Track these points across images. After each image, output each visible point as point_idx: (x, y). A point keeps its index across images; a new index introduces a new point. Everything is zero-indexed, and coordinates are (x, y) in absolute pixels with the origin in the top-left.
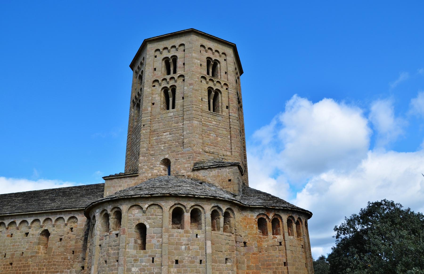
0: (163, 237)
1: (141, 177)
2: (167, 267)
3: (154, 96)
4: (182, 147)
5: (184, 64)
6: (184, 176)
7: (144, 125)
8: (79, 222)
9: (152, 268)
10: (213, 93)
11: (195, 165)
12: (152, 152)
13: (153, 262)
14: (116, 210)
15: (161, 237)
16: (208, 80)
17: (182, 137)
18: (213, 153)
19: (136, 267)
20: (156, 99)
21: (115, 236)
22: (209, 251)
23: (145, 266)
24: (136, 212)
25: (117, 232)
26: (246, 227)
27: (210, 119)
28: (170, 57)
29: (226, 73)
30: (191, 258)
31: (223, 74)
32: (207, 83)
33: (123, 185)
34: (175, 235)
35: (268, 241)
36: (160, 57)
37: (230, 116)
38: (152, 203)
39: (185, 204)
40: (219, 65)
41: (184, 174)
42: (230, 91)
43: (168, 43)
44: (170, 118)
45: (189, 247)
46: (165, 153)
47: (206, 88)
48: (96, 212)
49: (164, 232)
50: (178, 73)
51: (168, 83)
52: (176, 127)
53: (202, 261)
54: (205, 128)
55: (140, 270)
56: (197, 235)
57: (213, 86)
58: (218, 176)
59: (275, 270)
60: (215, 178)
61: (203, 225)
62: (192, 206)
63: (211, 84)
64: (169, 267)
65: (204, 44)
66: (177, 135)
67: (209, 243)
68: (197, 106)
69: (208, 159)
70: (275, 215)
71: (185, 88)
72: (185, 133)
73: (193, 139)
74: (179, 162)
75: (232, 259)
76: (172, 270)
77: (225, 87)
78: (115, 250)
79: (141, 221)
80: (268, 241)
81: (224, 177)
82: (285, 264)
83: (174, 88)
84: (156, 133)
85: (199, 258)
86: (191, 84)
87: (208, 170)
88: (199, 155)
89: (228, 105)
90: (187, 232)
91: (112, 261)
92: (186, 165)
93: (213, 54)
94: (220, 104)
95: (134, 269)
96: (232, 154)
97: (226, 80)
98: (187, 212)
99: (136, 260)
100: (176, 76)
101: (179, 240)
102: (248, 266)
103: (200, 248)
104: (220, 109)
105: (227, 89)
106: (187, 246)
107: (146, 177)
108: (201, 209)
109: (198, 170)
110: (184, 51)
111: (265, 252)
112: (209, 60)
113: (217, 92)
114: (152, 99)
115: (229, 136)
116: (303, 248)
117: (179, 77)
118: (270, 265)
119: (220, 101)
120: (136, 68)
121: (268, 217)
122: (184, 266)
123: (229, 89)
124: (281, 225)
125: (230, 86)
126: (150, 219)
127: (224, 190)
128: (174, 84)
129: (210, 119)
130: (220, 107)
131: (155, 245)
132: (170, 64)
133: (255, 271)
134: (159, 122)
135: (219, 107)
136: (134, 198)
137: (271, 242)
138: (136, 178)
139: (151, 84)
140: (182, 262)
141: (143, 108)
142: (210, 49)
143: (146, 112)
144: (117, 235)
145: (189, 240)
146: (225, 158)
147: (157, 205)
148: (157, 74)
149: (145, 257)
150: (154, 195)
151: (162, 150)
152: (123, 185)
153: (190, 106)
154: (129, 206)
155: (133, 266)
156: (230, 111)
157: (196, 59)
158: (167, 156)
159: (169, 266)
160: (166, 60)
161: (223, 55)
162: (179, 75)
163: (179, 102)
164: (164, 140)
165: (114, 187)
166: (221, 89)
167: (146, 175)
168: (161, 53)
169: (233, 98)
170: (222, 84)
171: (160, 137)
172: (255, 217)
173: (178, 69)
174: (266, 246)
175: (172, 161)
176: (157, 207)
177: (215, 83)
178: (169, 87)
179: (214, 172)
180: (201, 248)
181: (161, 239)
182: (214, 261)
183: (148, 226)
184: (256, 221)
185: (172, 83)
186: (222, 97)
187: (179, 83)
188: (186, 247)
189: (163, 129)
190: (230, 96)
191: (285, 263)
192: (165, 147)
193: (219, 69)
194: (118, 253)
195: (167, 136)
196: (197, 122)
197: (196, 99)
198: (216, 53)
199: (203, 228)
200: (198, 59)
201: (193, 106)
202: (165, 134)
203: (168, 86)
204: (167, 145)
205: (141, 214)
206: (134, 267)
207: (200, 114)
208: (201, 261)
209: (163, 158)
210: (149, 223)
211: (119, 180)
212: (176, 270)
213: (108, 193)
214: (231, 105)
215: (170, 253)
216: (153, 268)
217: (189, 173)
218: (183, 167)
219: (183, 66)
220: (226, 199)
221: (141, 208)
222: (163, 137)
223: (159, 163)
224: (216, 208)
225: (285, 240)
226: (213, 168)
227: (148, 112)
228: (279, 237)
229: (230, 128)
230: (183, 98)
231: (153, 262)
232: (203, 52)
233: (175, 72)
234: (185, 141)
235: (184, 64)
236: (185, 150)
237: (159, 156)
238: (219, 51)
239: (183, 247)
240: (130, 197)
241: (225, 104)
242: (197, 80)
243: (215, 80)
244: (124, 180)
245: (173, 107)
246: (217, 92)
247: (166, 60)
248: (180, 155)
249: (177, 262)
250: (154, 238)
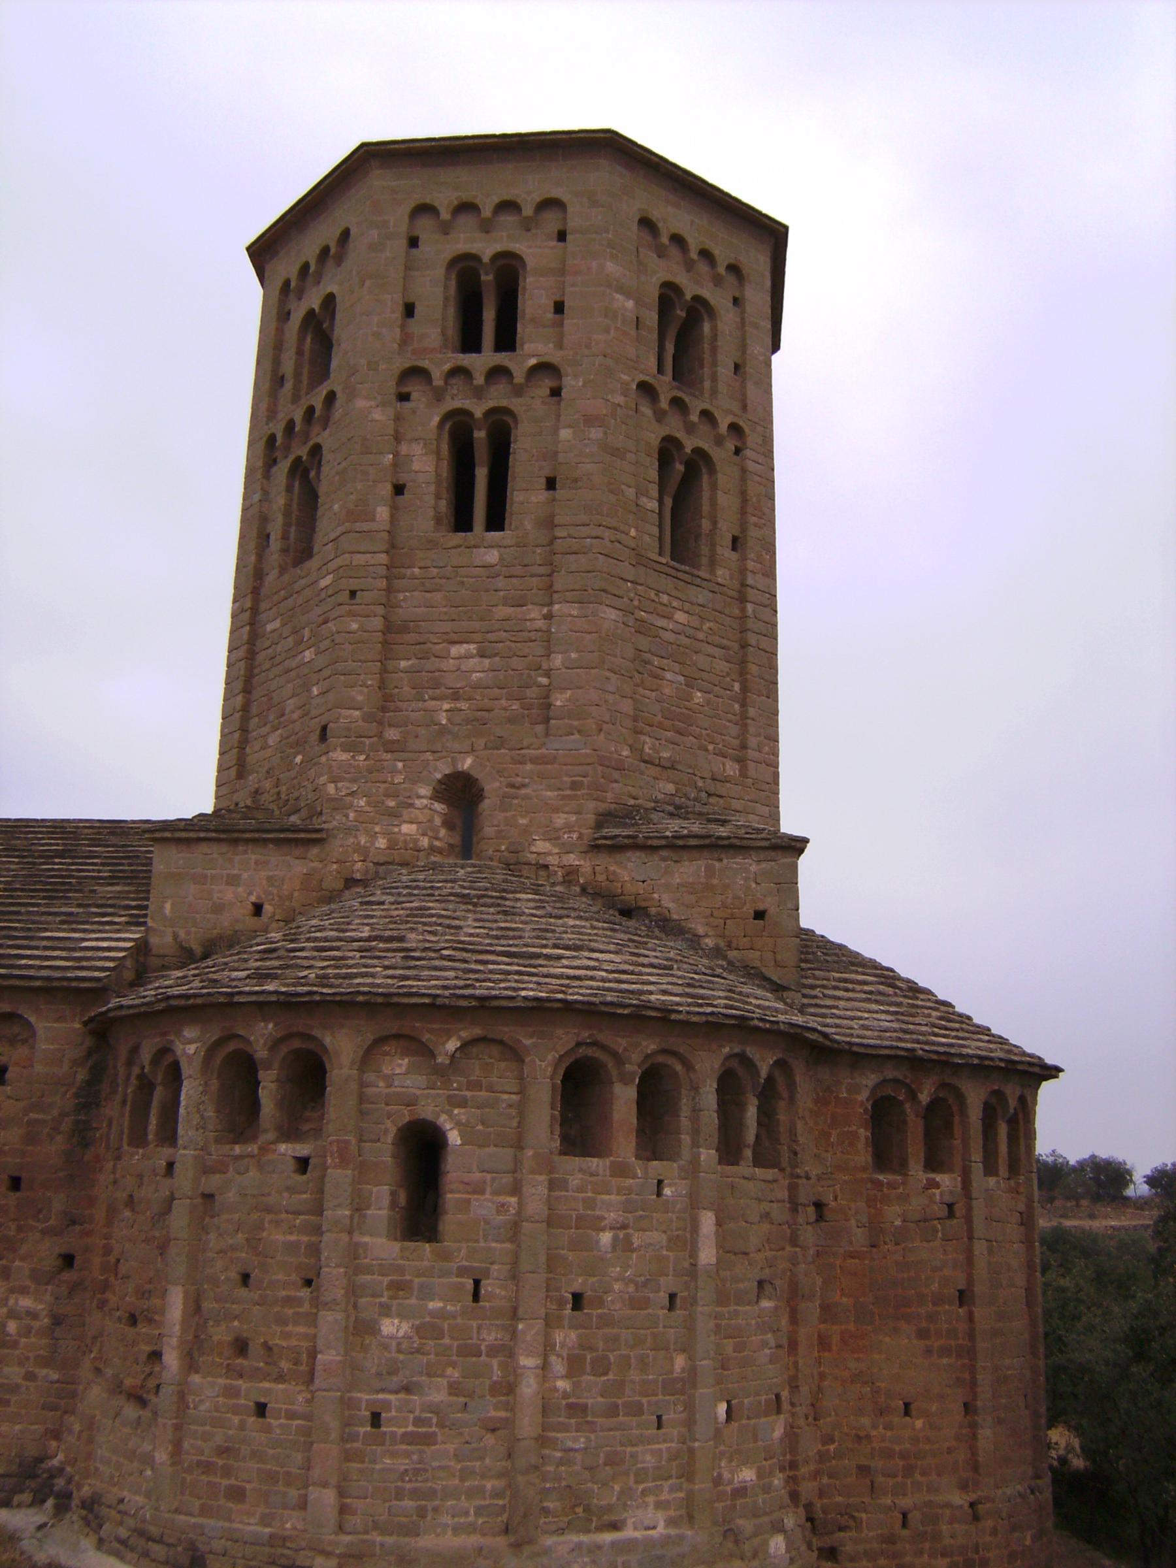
0: (527, 1190)
1: (337, 846)
2: (539, 1325)
4: (540, 728)
5: (559, 308)
6: (546, 867)
7: (353, 594)
8: (43, 1046)
9: (474, 1324)
10: (680, 467)
11: (599, 825)
13: (476, 1297)
14: (297, 1044)
15: (516, 1189)
16: (664, 404)
17: (544, 681)
18: (673, 768)
19: (402, 1316)
20: (416, 466)
21: (291, 1165)
22: (707, 1255)
23: (441, 1314)
24: (398, 1067)
25: (303, 1149)
26: (829, 1135)
27: (665, 598)
28: (486, 259)
29: (737, 367)
30: (636, 1284)
31: (725, 371)
32: (660, 416)
33: (245, 875)
34: (575, 1181)
35: (904, 1199)
36: (439, 250)
38: (477, 1031)
39: (620, 1043)
40: (707, 327)
41: (552, 860)
45: (628, 1240)
46: (457, 746)
48: (179, 1033)
49: (533, 1172)
50: (528, 347)
53: (678, 1301)
54: (644, 642)
55: (418, 1329)
56: (660, 1182)
57: (680, 435)
58: (709, 887)
59: (924, 1324)
60: (693, 898)
61: (686, 1139)
62: (647, 1057)
63: (674, 427)
64: (547, 1325)
65: (655, 214)
66: (515, 662)
67: (708, 1221)
68: (622, 537)
70: (943, 1085)
71: (565, 434)
72: (558, 660)
74: (526, 797)
75: (778, 1282)
76: (558, 1336)
78: (292, 1229)
79: (426, 1111)
80: (904, 1199)
81: (736, 897)
82: (963, 1297)
84: (411, 637)
85: (668, 1283)
86: (590, 420)
87: (664, 853)
88: (616, 775)
90: (621, 1170)
91: (280, 1276)
92: (560, 820)
93: (689, 266)
94: (706, 524)
95: (389, 1327)
96: (744, 773)
97: (735, 407)
98: (625, 1080)
99: (399, 1287)
101: (590, 1204)
102: (826, 1308)
103: (669, 1240)
104: (705, 550)
105: (737, 451)
106: (621, 1234)
107: (358, 848)
108: (679, 1068)
109: (616, 848)
110: (562, 236)
111: (890, 1247)
112: (669, 294)
113: (699, 462)
114: (395, 464)
115: (737, 687)
116: (1022, 1224)
119: (706, 507)
120: (286, 267)
121: (913, 1096)
122: (606, 1321)
123: (748, 453)
124: (957, 1130)
126: (463, 1103)
127: (732, 954)
128: (504, 403)
129: (665, 598)
131: (487, 1222)
133: (852, 1327)
135: (698, 537)
136: (398, 1004)
137: (917, 1203)
138: (314, 851)
139: (391, 387)
140: (601, 1303)
142: (678, 240)
143: (365, 526)
144: (303, 1164)
145: (628, 1207)
146: (722, 789)
147: (501, 1042)
149: (445, 1273)
150: (495, 1003)
151: (443, 731)
153: (585, 531)
154: (371, 1037)
155: (386, 1311)
156: (751, 565)
157: (621, 290)
158: (467, 763)
159: (550, 1322)
160: (465, 269)
161: (731, 279)
162: (533, 361)
163: (526, 497)
165: (200, 879)
166: (716, 453)
167: (363, 840)
170: (723, 427)
171: (429, 664)
172: (864, 1095)
173: (523, 330)
174: (898, 1223)
175: (492, 787)
176: (495, 1050)
177: (694, 418)
178: (478, 413)
179: (690, 870)
180: (675, 1242)
181: (513, 1200)
182: (722, 1298)
183: (454, 1138)
184: (866, 1110)
185: (498, 396)
186: (714, 487)
187: (531, 408)
188: (615, 1239)
189: (447, 627)
194: (314, 1250)
195: (464, 660)
196: (612, 614)
198: (703, 267)
199: (686, 1154)
200: (628, 294)
201: (599, 531)
202: (455, 650)
204: (464, 705)
205: (421, 1080)
206: (388, 1315)
207: (630, 573)
208: (672, 1297)
209: (442, 769)
210: (458, 1124)
211: (224, 848)
212: (573, 1335)
213: (168, 906)
215: (552, 1263)
216: (479, 1327)
217: (572, 859)
219: (550, 315)
220: (782, 1027)
221: (428, 1053)
223: (425, 791)
224: (734, 1063)
226: (684, 847)
228: (947, 1181)
230: (551, 484)
231: (476, 1297)
232: (651, 258)
233: (507, 340)
234: (559, 700)
235: (559, 308)
237: (429, 756)
238: (716, 251)
239: (606, 1238)
240: (380, 1000)
241: (727, 528)
242: (619, 399)
243: (696, 406)
244: (253, 855)
245: (496, 521)
246: (699, 462)
247: (465, 269)
248: (529, 767)
249: (578, 1300)
250: (482, 1192)
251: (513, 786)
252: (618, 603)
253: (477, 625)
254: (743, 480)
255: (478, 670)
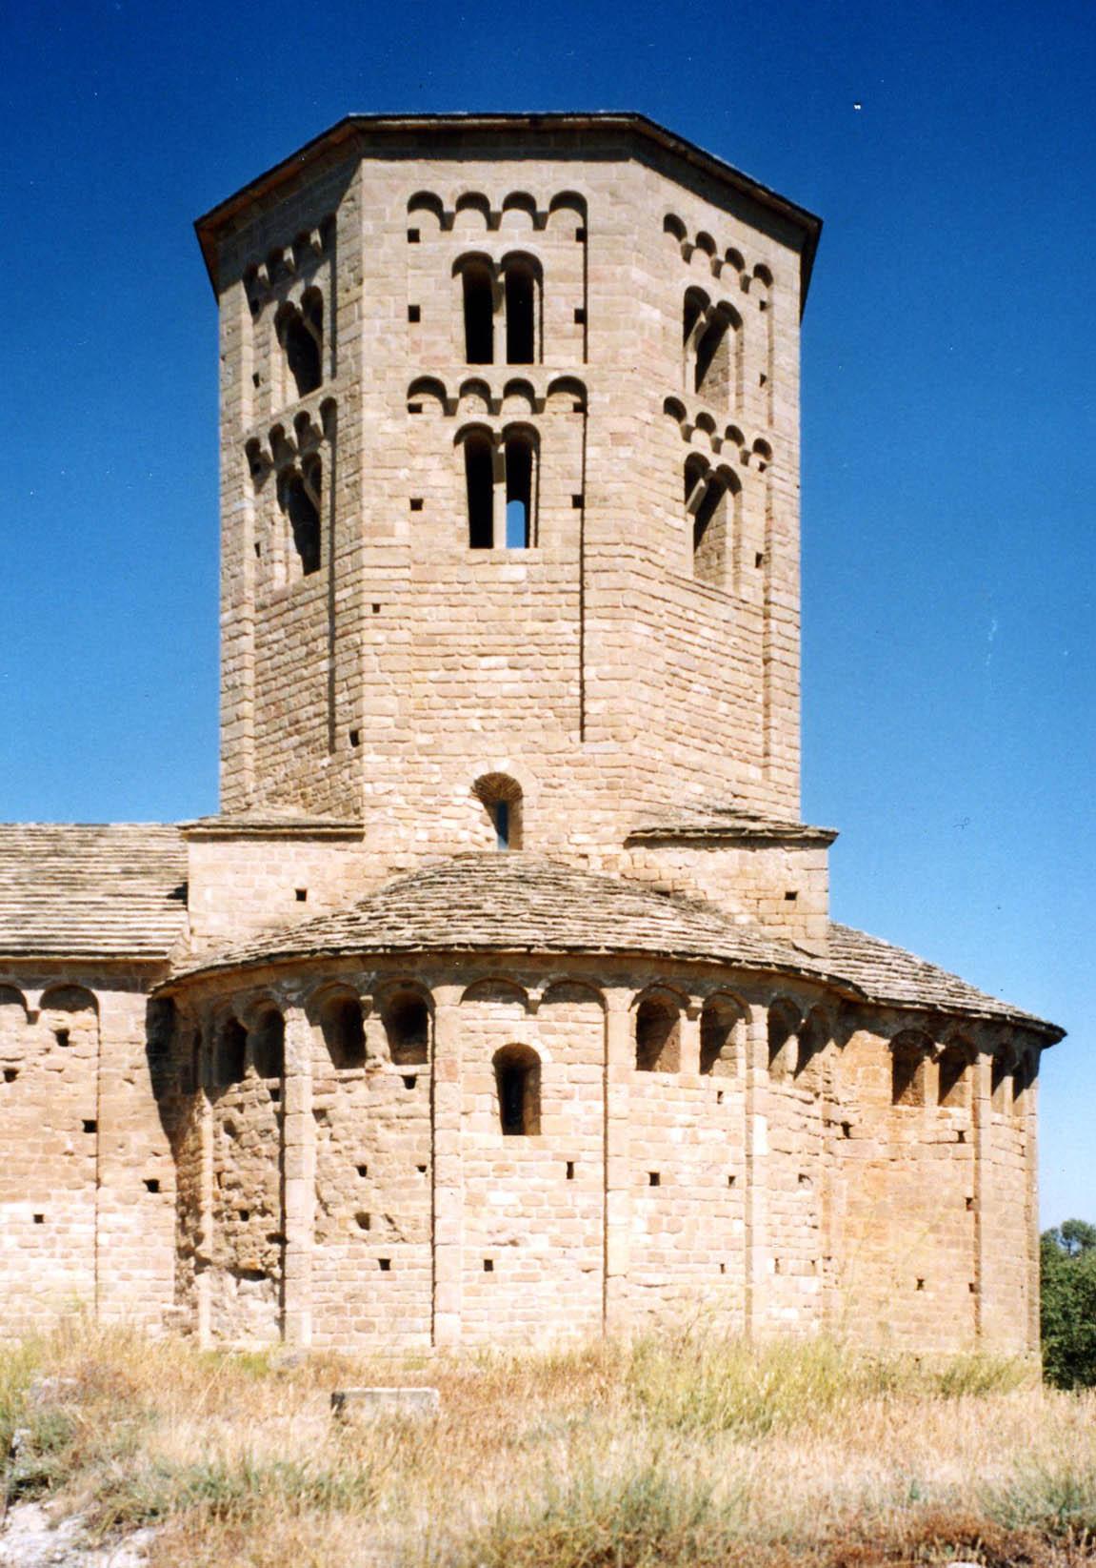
3: (419, 462)
12: (423, 739)
27: (691, 615)
36: (444, 247)
37: (767, 602)
42: (776, 483)
43: (496, 178)
44: (511, 588)
46: (491, 750)
47: (682, 459)
51: (494, 408)
52: (543, 639)
69: (688, 799)
73: (629, 705)
77: (756, 460)
83: (523, 443)
89: (762, 551)
100: (540, 377)
105: (762, 468)
117: (557, 386)
118: (921, 1205)
125: (778, 455)
130: (728, 558)
132: (500, 300)
134: (454, 600)
138: (355, 845)
141: (367, 516)
148: (434, 343)
152: (286, 866)
158: (503, 766)
162: (555, 375)
164: (481, 689)
168: (446, 223)
169: (788, 517)
175: (530, 788)
178: (497, 429)
185: (516, 410)
186: (739, 506)
187: (555, 423)
189: (477, 640)
190: (778, 506)
191: (969, 1200)
192: (491, 724)
193: (732, 359)
197: (643, 518)
202: (485, 662)
203: (497, 425)
214: (777, 550)
218: (576, 824)
222: (474, 675)
223: (465, 790)
225: (978, 1127)
227: (393, 541)
229: (766, 662)
233: (521, 350)
236: (587, 747)
237: (465, 758)
241: (752, 546)
248: (566, 768)
251: (551, 786)
252: (647, 618)
253: (508, 639)
254: (769, 498)
255: (509, 682)
